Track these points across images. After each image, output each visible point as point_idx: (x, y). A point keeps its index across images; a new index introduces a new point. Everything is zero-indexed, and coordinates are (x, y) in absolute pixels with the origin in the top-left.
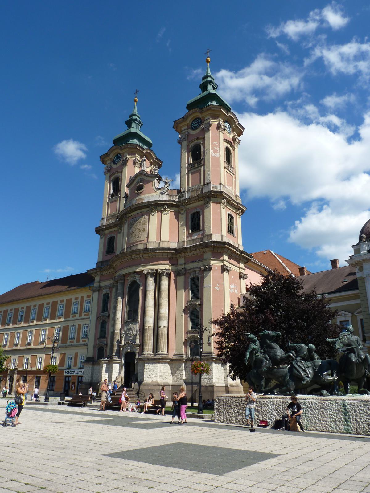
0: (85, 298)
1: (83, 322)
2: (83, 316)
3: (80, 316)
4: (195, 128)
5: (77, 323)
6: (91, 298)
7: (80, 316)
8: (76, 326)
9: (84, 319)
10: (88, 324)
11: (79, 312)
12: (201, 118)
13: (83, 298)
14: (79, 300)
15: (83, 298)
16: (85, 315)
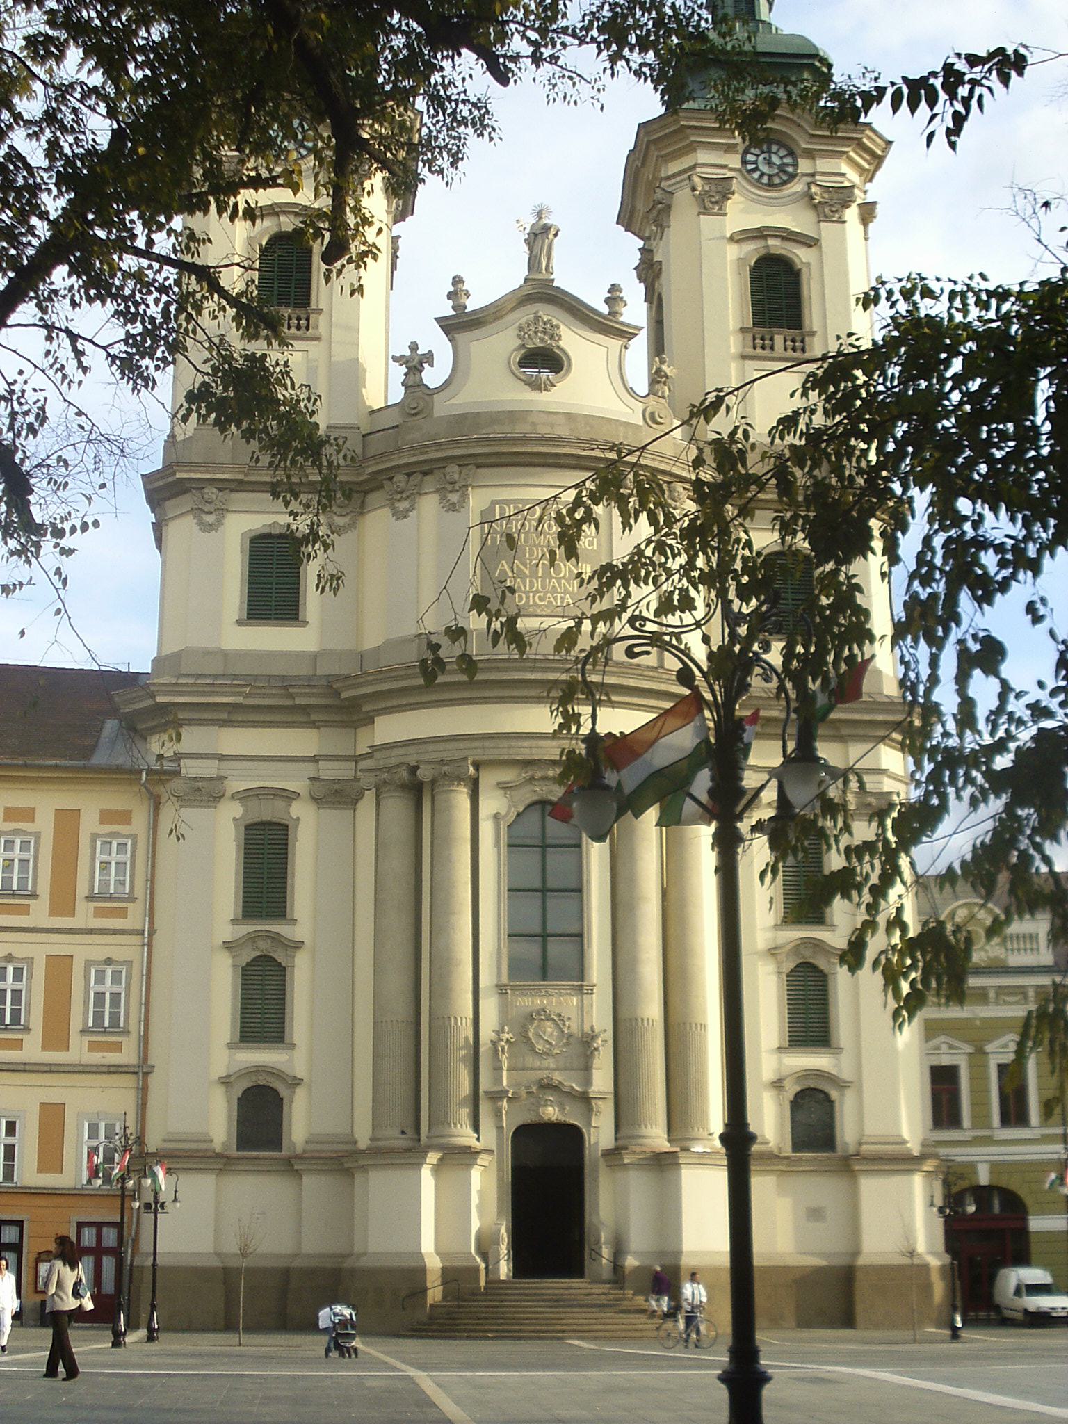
0: (89, 823)
1: (82, 951)
2: (84, 915)
3: (54, 912)
4: (765, 180)
5: (37, 950)
6: (139, 823)
7: (54, 912)
8: (30, 961)
9: (91, 932)
10: (129, 963)
11: (44, 888)
12: (798, 152)
13: (67, 822)
14: (45, 823)
15: (67, 822)
16: (99, 913)
